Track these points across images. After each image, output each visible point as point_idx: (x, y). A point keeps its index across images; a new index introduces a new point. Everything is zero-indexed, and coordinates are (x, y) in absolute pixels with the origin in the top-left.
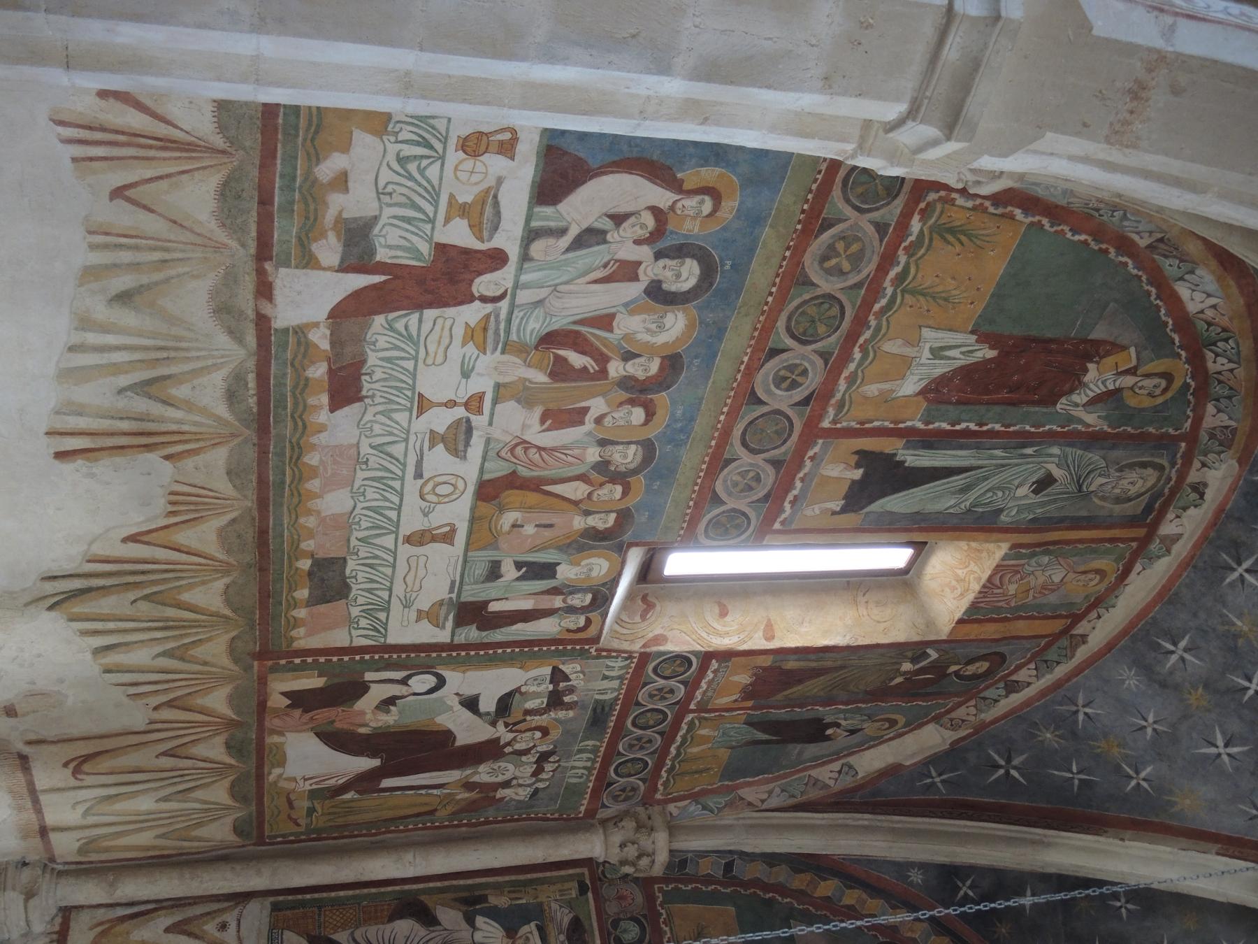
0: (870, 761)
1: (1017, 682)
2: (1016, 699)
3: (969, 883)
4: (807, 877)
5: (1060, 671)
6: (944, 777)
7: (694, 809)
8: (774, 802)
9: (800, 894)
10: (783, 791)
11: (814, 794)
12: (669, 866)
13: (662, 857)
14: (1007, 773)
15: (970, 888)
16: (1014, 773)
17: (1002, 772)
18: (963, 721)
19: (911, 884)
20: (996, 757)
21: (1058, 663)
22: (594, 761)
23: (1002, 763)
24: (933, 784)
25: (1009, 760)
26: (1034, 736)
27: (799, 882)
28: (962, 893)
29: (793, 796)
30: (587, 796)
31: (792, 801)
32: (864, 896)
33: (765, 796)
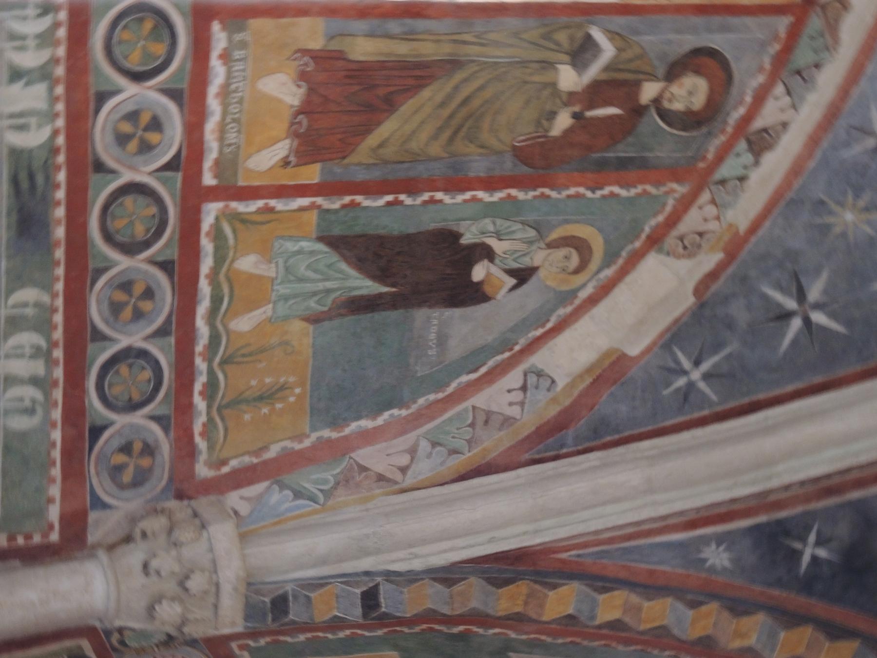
0: (570, 356)
1: (765, 130)
2: (776, 163)
3: (812, 538)
4: (522, 588)
5: (829, 79)
6: (705, 366)
7: (278, 498)
8: (423, 469)
9: (517, 620)
10: (435, 444)
11: (494, 443)
12: (251, 611)
13: (230, 574)
14: (807, 321)
15: (819, 543)
16: (819, 318)
17: (796, 323)
18: (701, 234)
19: (712, 570)
20: (778, 296)
21: (817, 66)
22: (51, 362)
23: (791, 304)
24: (691, 385)
25: (801, 296)
26: (825, 229)
27: (506, 601)
28: (806, 559)
29: (454, 452)
30: (56, 472)
31: (456, 463)
32: (634, 598)
33: (404, 460)
